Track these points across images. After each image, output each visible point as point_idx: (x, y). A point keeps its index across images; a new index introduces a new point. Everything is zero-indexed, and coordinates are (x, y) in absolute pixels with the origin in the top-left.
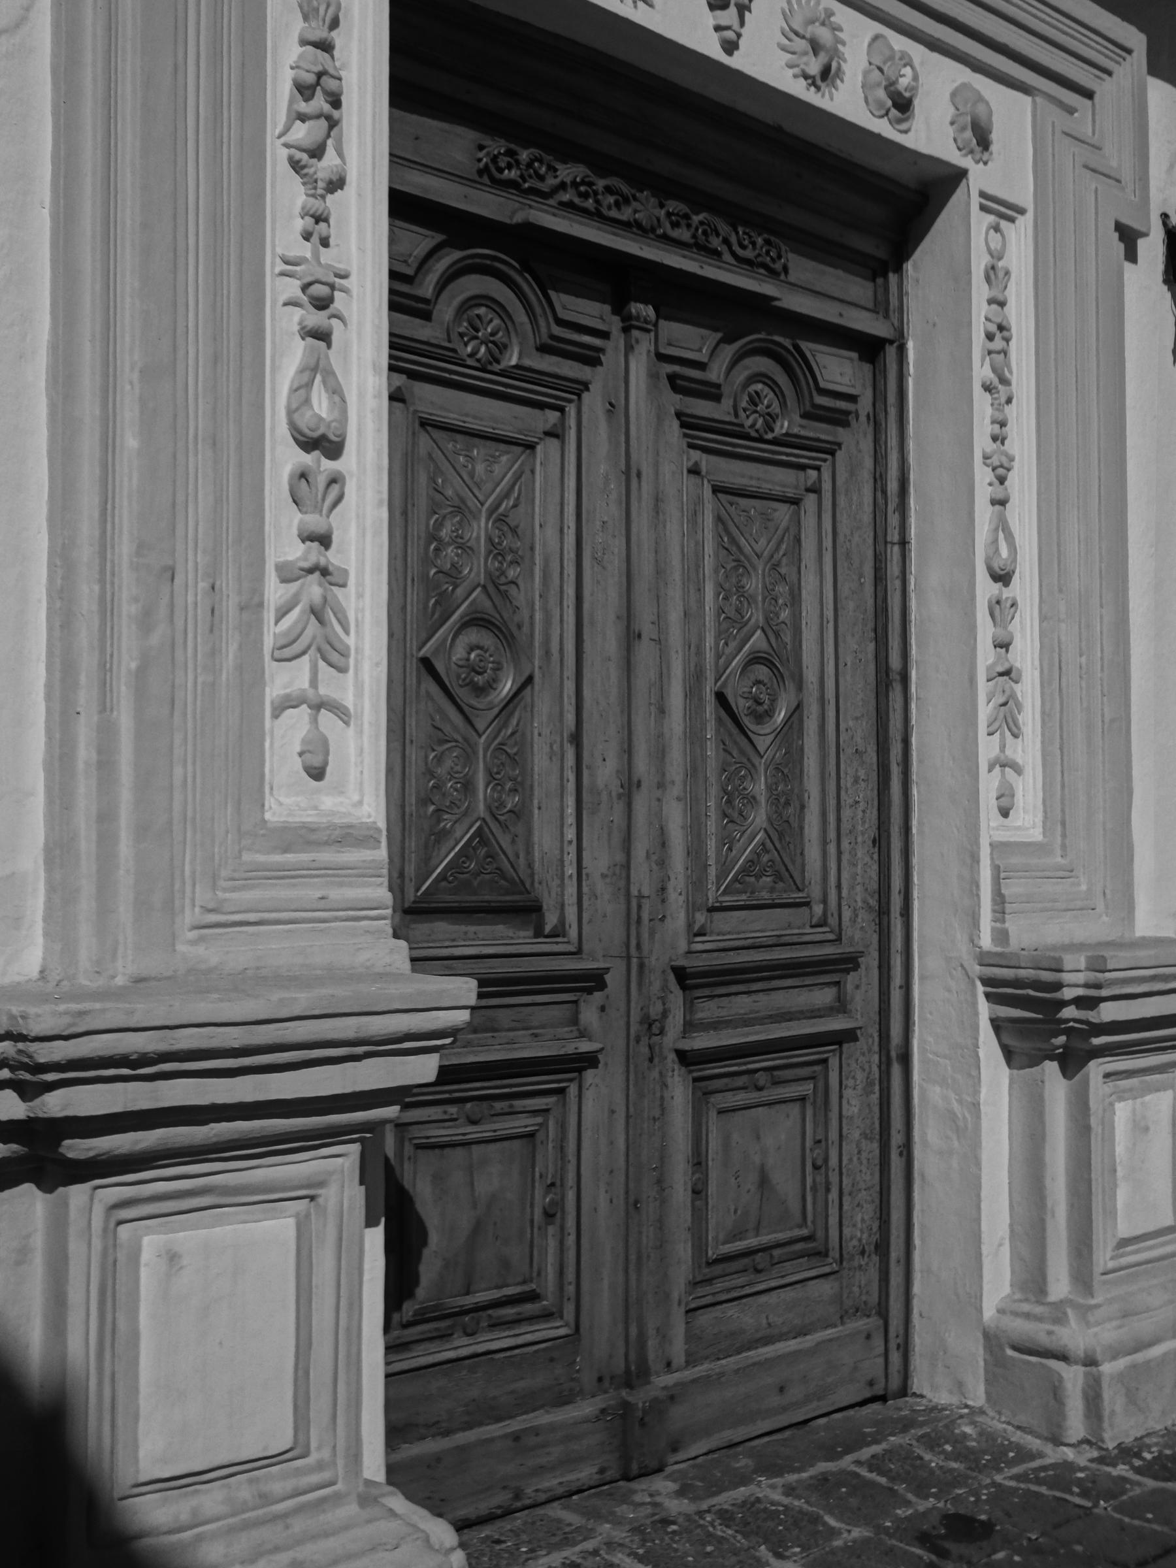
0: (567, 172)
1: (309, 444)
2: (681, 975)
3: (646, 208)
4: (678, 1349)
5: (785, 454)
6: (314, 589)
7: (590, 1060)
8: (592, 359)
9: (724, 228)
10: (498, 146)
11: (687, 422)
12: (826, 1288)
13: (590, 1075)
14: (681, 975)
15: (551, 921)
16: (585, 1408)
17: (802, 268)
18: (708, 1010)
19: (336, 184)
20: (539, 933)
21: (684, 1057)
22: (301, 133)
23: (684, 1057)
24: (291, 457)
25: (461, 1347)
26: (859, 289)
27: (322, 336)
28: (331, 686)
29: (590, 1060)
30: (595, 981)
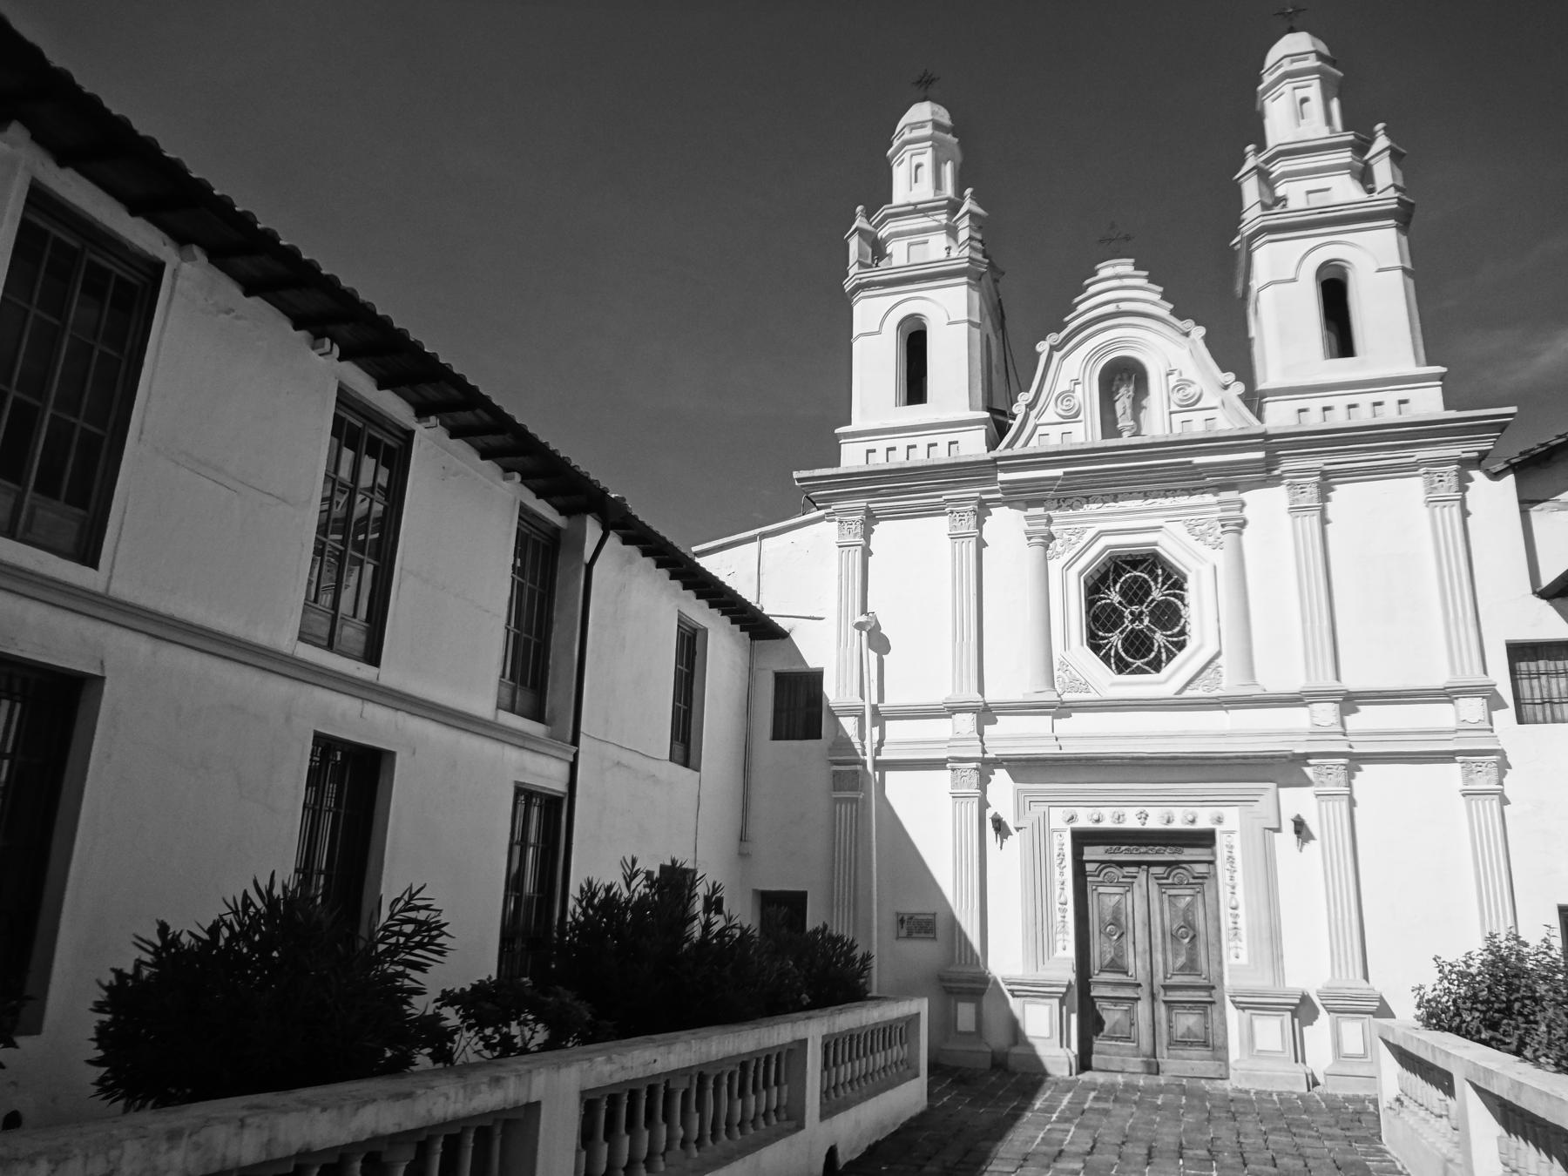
0: (1123, 848)
1: (1061, 904)
2: (1162, 986)
3: (1143, 849)
4: (1165, 1056)
5: (1189, 886)
6: (1062, 924)
7: (1139, 999)
8: (1135, 877)
9: (1164, 848)
10: (1108, 847)
11: (1159, 884)
12: (1209, 1053)
13: (1139, 1002)
14: (1162, 986)
15: (1130, 974)
16: (1139, 1059)
17: (1187, 851)
18: (1169, 993)
19: (1065, 867)
20: (1128, 975)
21: (1165, 1002)
22: (1059, 861)
23: (1165, 1002)
24: (1058, 906)
25: (1113, 1043)
26: (1207, 851)
27: (1063, 889)
28: (1066, 937)
29: (1139, 999)
30: (1139, 985)
